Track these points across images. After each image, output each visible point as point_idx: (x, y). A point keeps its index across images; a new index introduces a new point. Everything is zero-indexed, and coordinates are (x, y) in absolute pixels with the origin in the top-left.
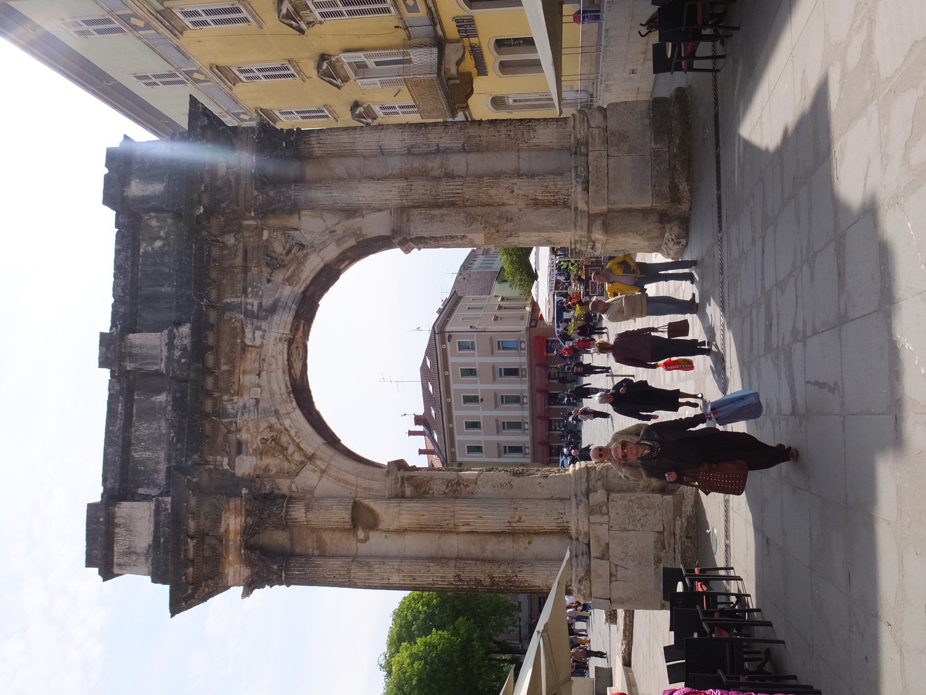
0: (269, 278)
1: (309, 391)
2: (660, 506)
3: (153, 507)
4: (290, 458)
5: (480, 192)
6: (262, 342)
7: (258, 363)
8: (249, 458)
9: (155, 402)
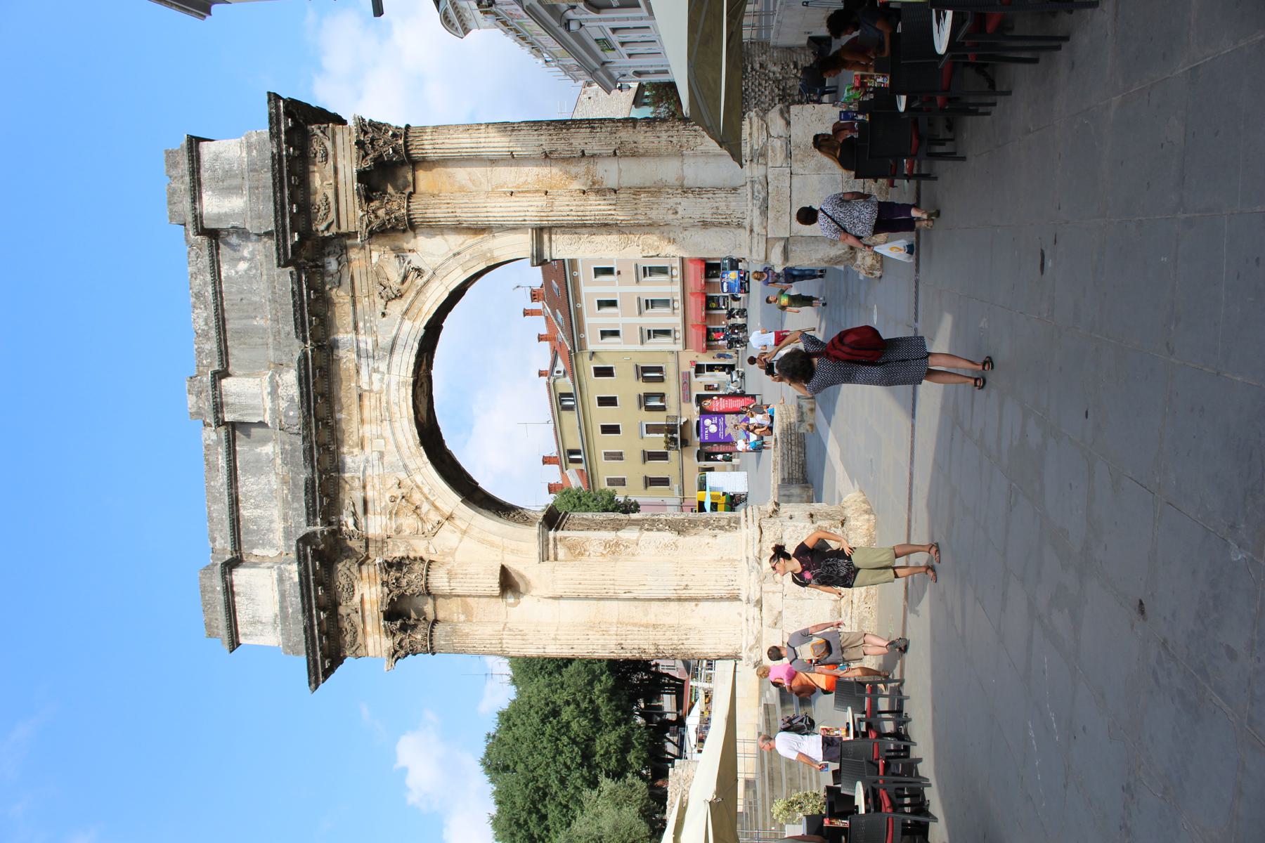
0: (383, 311)
1: (438, 429)
5: (636, 214)
6: (381, 387)
7: (378, 410)
8: (378, 517)
9: (260, 454)
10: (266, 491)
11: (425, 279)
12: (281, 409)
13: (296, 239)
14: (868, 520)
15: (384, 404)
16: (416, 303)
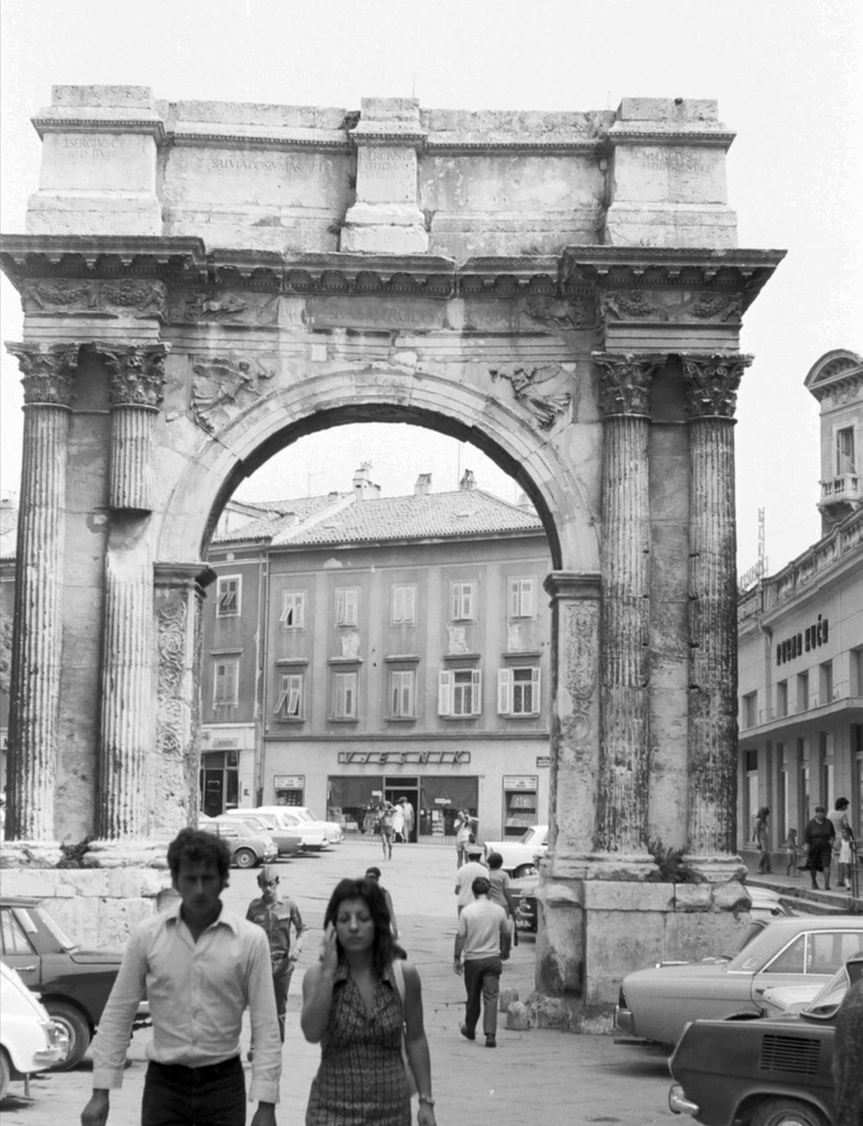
0: (499, 373)
1: (327, 427)
4: (215, 409)
11: (539, 432)
13: (600, 272)
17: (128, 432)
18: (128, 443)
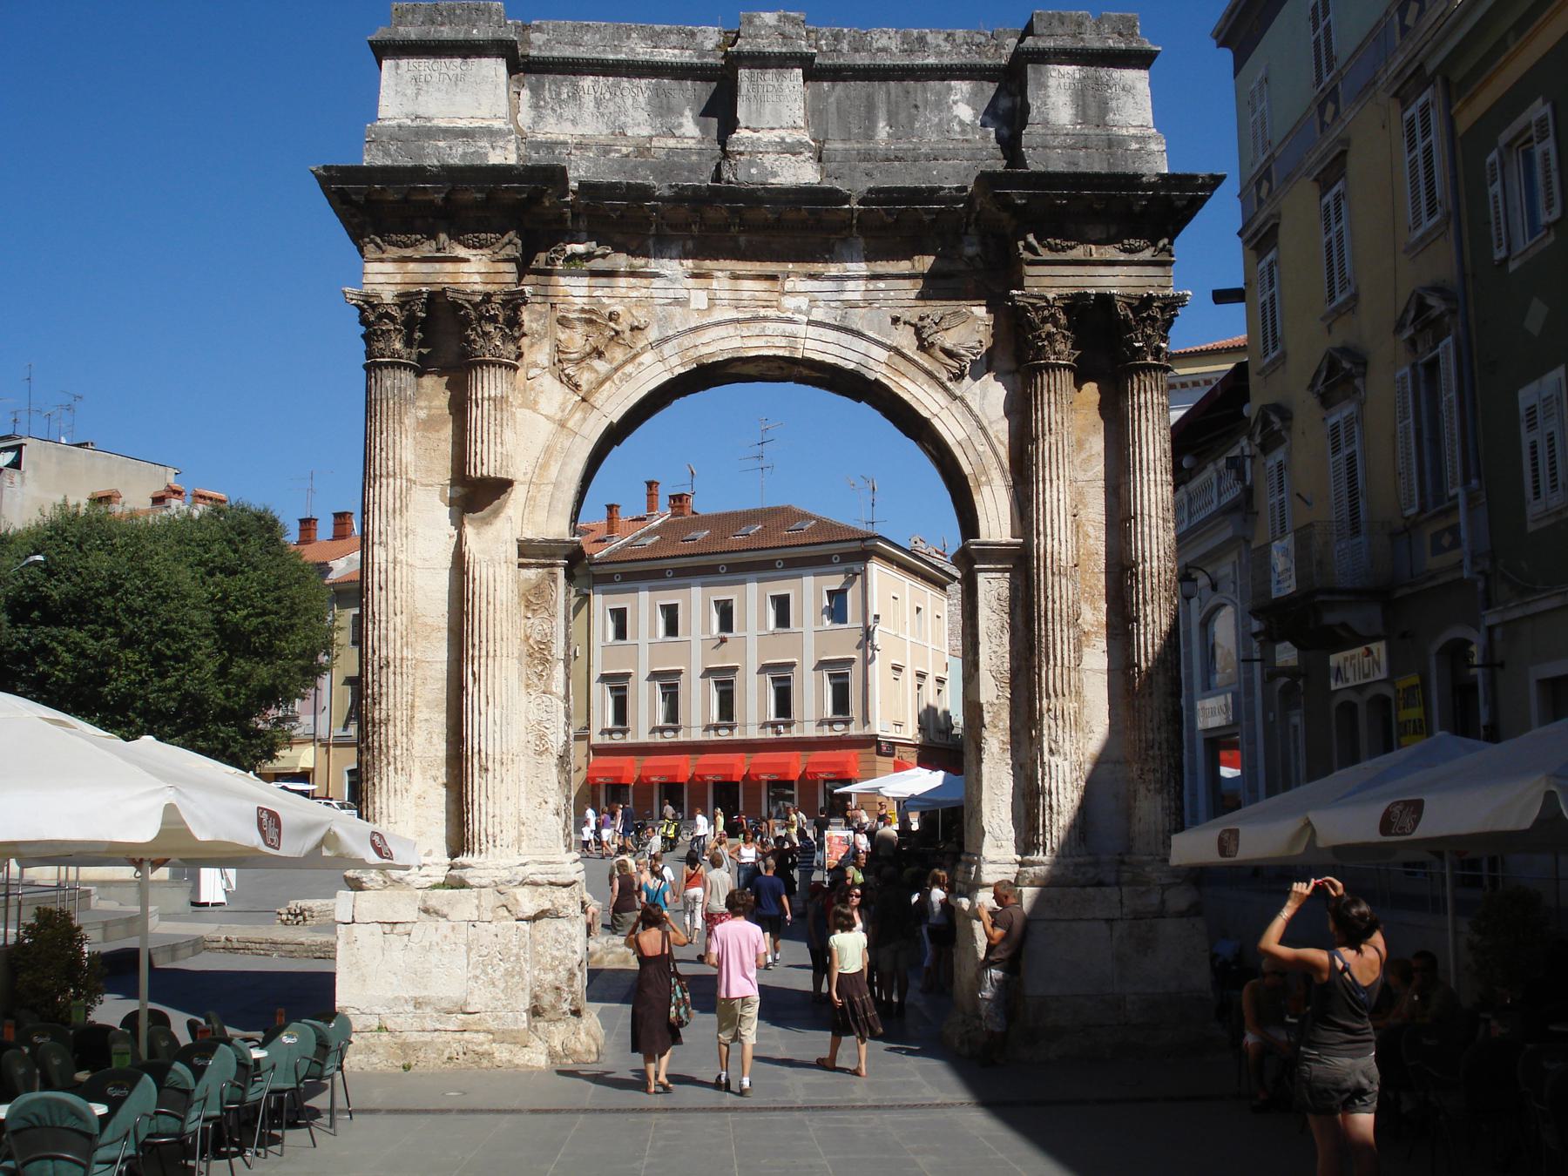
2: (510, 1007)
3: (498, 124)
4: (583, 364)
6: (788, 310)
9: (682, 115)
10: (622, 118)
12: (760, 156)
14: (590, 1052)
15: (762, 312)
16: (913, 368)
17: (486, 389)
18: (486, 403)
